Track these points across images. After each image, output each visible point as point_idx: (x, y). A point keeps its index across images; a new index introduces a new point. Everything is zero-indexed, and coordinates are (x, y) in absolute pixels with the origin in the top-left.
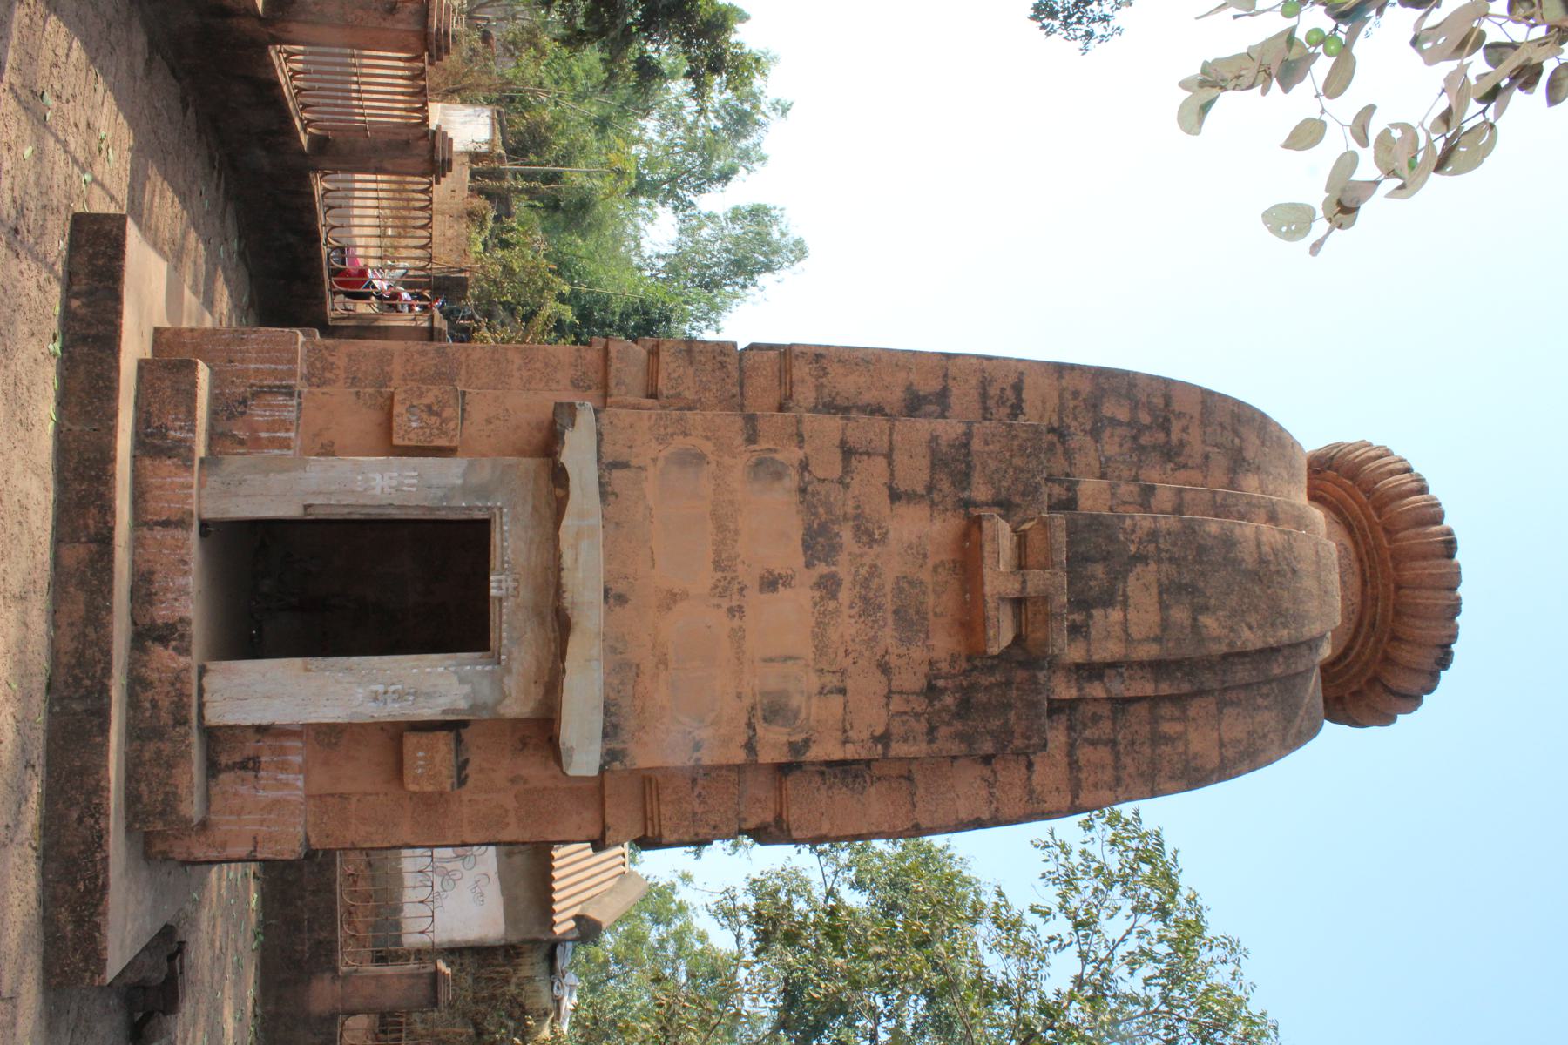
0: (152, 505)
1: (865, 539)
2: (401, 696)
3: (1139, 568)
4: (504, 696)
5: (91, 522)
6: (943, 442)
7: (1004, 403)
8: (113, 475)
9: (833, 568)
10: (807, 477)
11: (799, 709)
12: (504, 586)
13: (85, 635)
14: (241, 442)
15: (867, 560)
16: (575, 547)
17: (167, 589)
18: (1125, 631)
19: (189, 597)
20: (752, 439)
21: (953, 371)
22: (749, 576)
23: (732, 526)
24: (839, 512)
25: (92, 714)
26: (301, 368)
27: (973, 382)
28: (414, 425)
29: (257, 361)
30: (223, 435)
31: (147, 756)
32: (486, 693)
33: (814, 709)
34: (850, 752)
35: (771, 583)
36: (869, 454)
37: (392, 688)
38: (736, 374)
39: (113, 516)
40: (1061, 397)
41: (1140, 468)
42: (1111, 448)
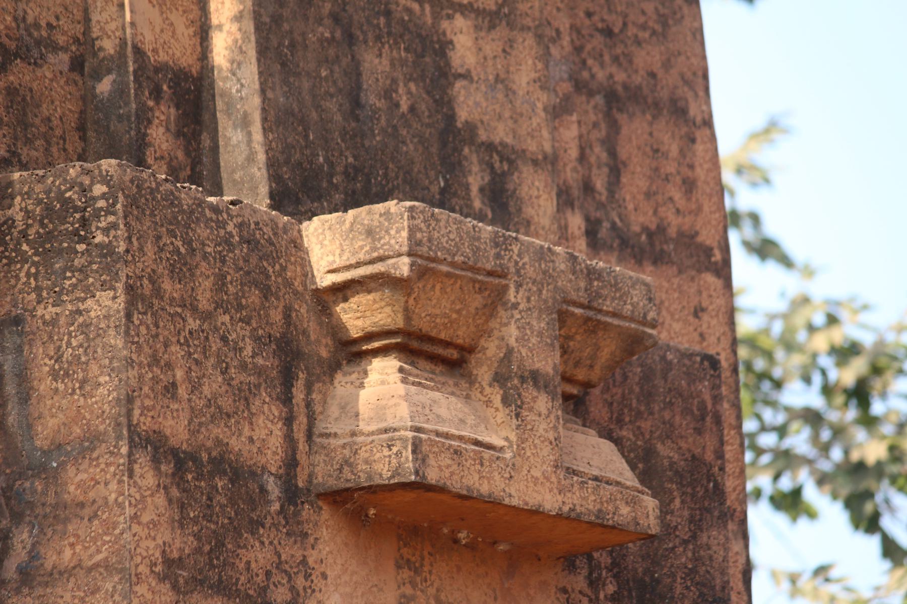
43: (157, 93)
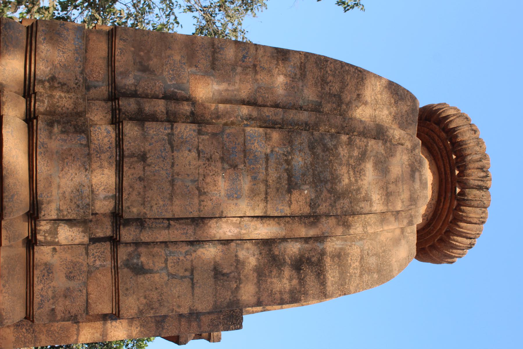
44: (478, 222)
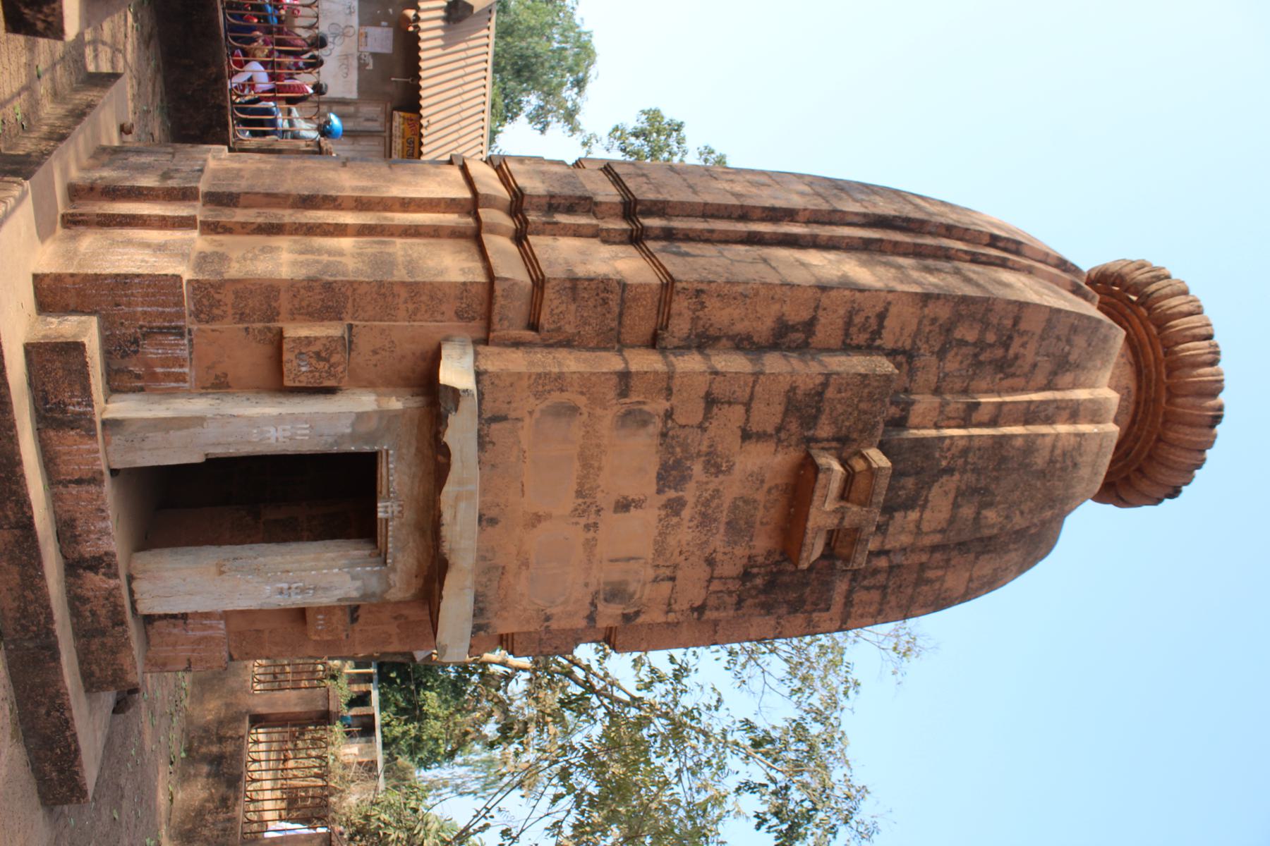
0: (63, 468)
1: (713, 470)
2: (303, 591)
3: (945, 478)
4: (390, 587)
5: (10, 513)
6: (800, 392)
7: (865, 330)
8: (22, 476)
9: (681, 493)
10: (670, 423)
11: (635, 592)
12: (390, 510)
13: (25, 597)
14: (138, 377)
15: (711, 486)
16: (455, 507)
17: (89, 532)
18: (918, 527)
19: (111, 532)
20: (624, 393)
21: (825, 301)
22: (605, 500)
23: (596, 464)
24: (693, 450)
25: (43, 648)
26: (188, 305)
27: (842, 312)
28: (304, 369)
29: (143, 304)
30: (118, 371)
31: (94, 647)
32: (374, 585)
33: (647, 591)
34: (671, 617)
35: (624, 506)
36: (730, 403)
37: (295, 585)
38: (616, 310)
39: (30, 507)
40: (920, 323)
41: (972, 379)
42: (952, 364)
43: (903, 410)
44: (1192, 308)
